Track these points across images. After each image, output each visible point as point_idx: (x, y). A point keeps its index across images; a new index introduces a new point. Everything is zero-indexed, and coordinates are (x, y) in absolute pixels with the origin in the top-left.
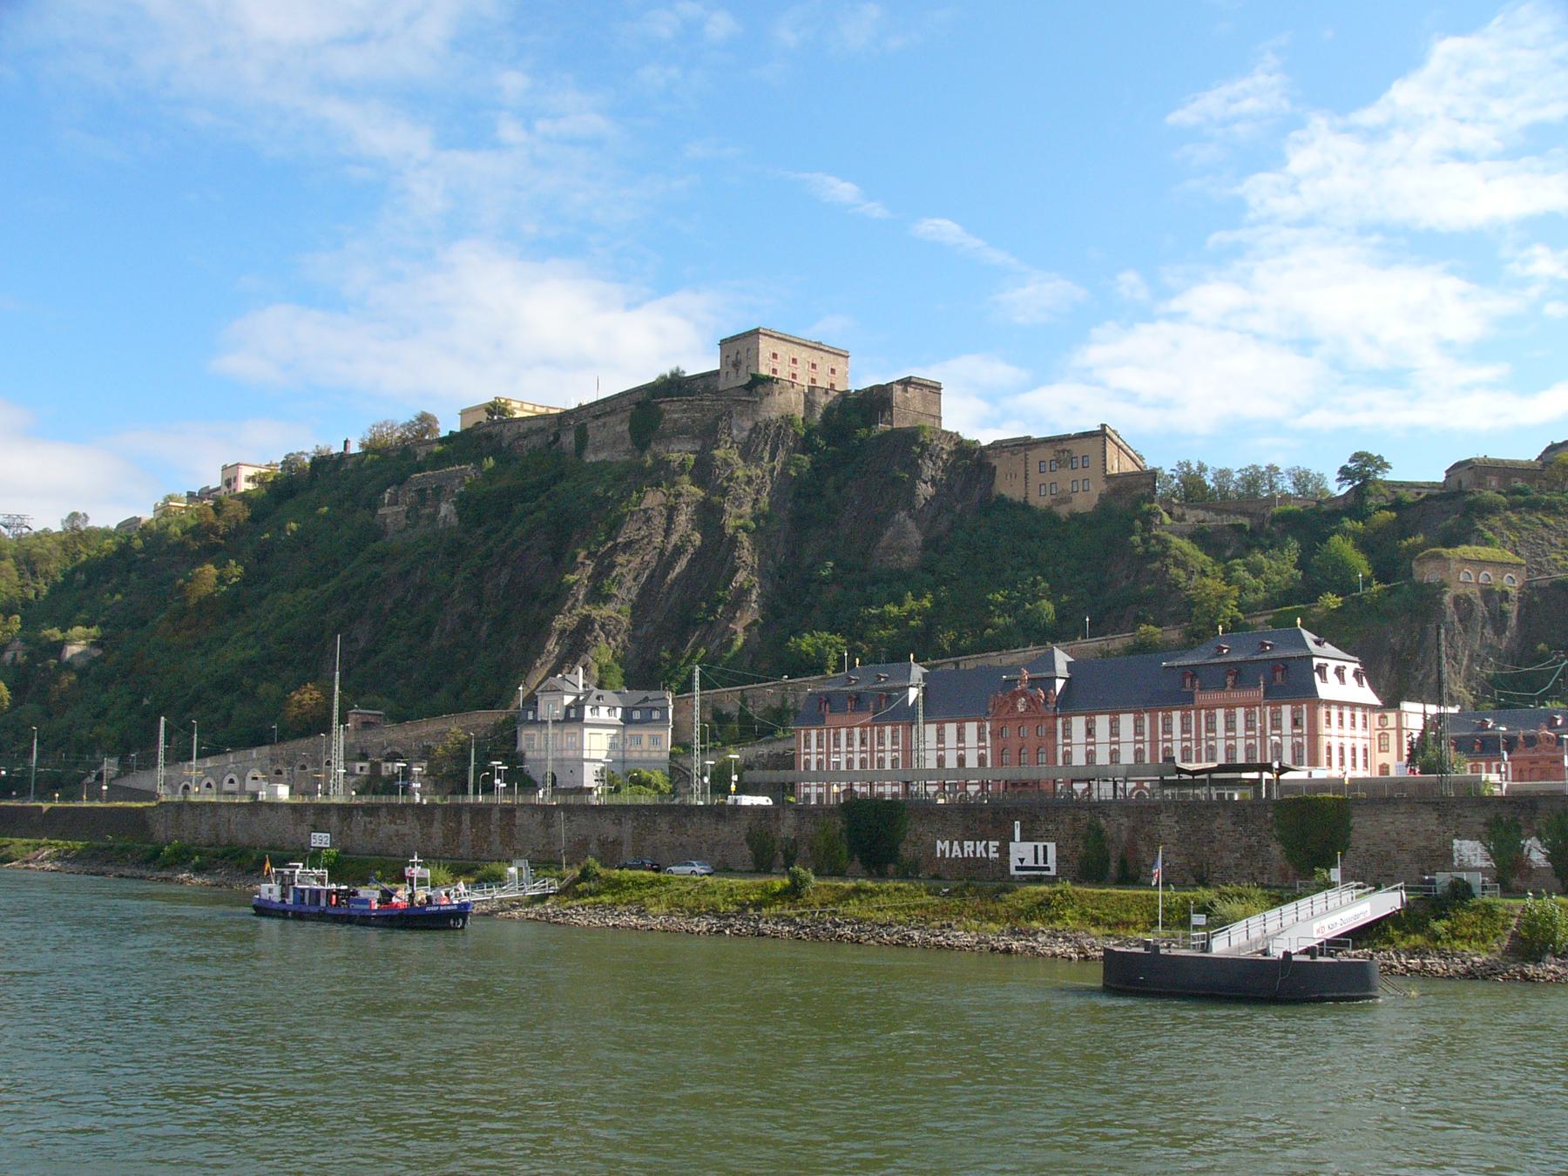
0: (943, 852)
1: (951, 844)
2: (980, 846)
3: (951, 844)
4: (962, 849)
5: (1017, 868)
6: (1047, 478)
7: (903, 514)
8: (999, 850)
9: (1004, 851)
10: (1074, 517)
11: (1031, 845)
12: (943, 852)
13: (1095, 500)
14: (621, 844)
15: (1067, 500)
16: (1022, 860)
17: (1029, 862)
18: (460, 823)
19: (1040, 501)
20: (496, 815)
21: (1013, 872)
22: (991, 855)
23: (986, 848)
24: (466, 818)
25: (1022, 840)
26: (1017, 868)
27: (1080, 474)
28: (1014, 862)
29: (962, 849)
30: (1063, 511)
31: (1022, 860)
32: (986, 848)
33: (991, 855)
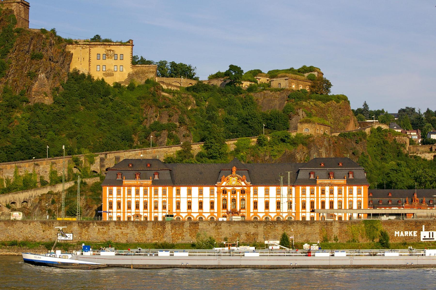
0: (397, 235)
1: (400, 232)
2: (410, 233)
3: (400, 232)
4: (404, 234)
5: (423, 239)
6: (102, 62)
7: (42, 75)
8: (417, 234)
9: (419, 234)
10: (117, 85)
11: (428, 232)
12: (397, 235)
13: (126, 77)
14: (257, 235)
15: (110, 75)
16: (425, 237)
17: (427, 237)
18: (164, 228)
19: (97, 75)
20: (187, 225)
21: (422, 240)
22: (414, 235)
23: (413, 233)
24: (168, 227)
25: (425, 231)
26: (423, 239)
27: (119, 62)
28: (422, 237)
29: (404, 234)
30: (110, 81)
31: (425, 237)
32: (413, 233)
33: (414, 235)
